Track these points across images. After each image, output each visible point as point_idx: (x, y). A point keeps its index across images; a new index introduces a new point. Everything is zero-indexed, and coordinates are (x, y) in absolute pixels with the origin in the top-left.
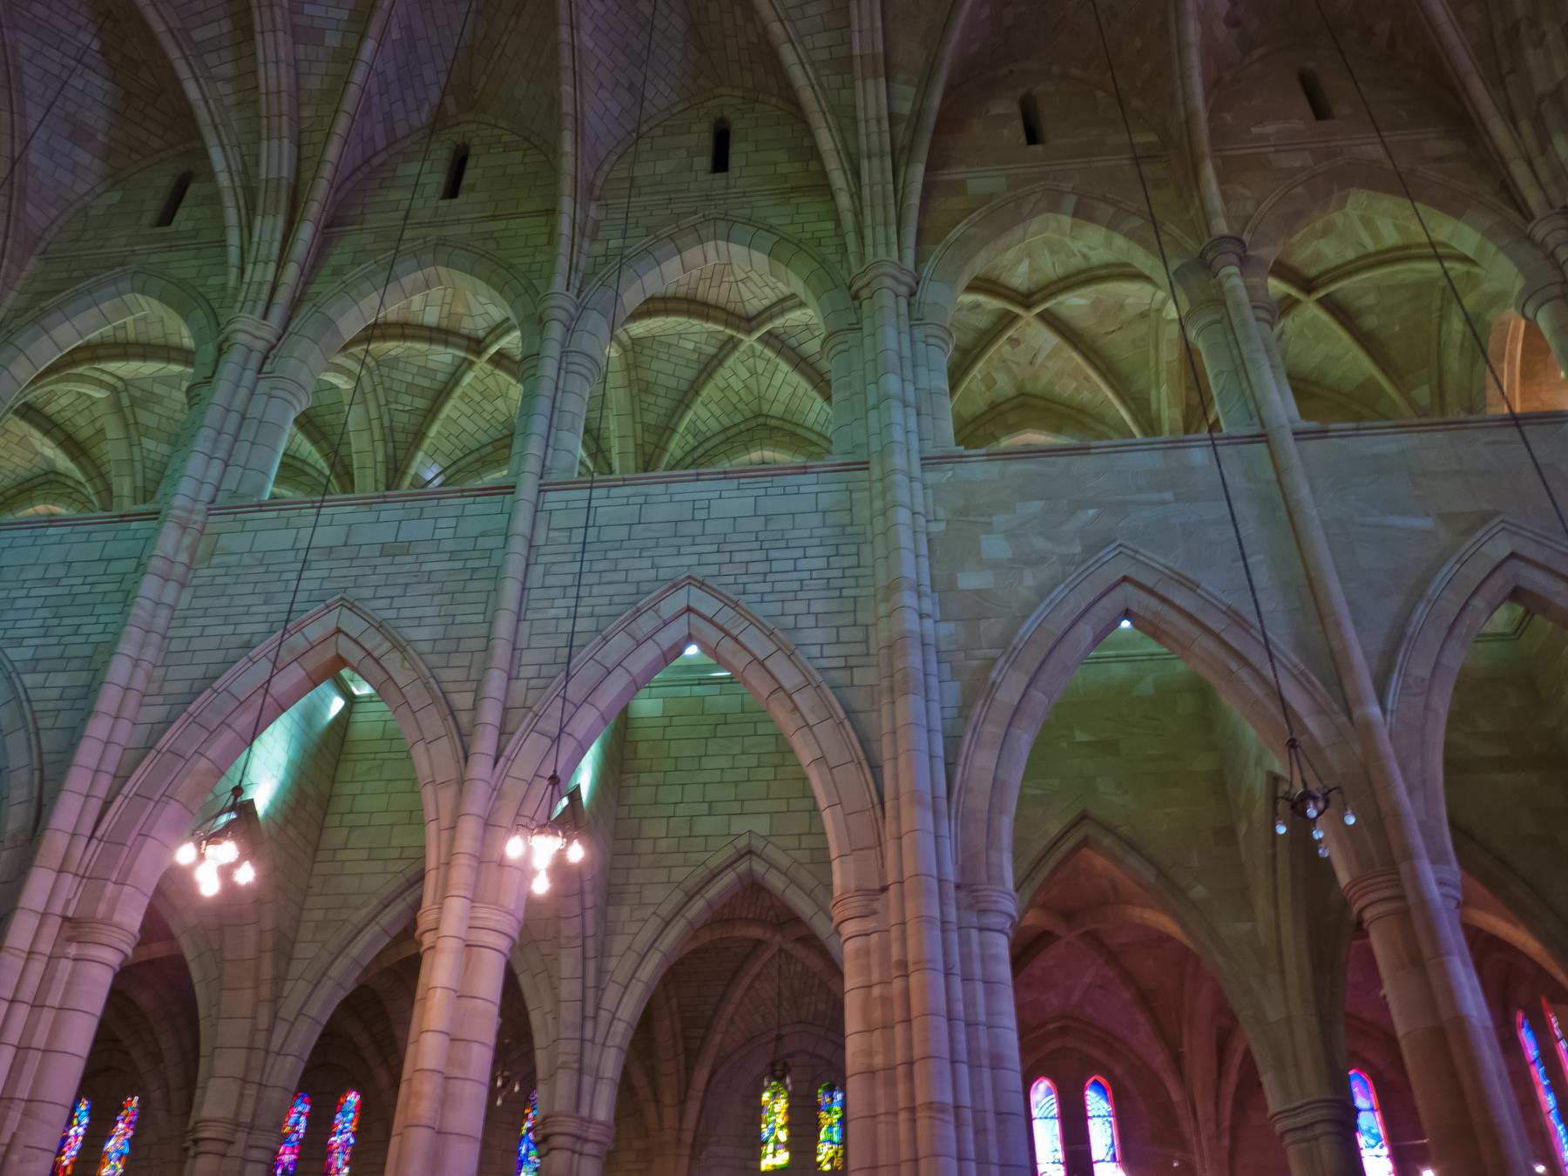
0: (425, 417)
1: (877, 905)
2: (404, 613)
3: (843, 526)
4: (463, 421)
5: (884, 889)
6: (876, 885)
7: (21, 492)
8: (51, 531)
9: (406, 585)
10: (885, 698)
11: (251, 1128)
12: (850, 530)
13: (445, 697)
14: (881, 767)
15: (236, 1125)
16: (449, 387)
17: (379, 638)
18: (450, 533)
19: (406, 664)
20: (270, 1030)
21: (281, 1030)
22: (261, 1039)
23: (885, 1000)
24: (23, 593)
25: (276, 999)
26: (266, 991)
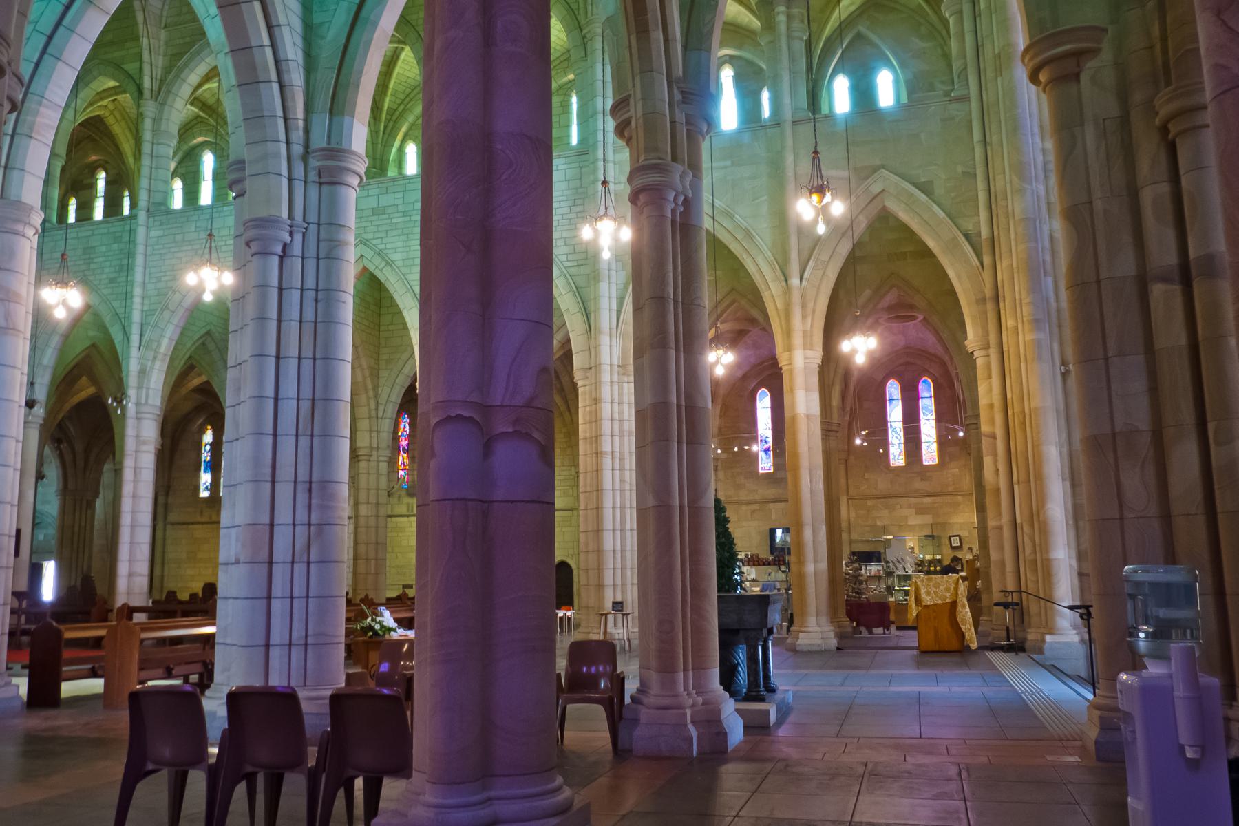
0: (386, 75)
1: (588, 375)
2: (389, 246)
3: (577, 189)
4: (407, 73)
5: (591, 368)
6: (587, 366)
7: (187, 130)
8: (225, 208)
9: (387, 231)
10: (592, 282)
11: (378, 448)
12: (580, 190)
13: (412, 288)
14: (590, 314)
15: (371, 448)
16: (394, 59)
17: (380, 260)
18: (401, 201)
19: (393, 272)
20: (377, 409)
21: (381, 409)
22: (373, 413)
23: (590, 412)
24: (223, 243)
25: (376, 396)
26: (371, 393)
